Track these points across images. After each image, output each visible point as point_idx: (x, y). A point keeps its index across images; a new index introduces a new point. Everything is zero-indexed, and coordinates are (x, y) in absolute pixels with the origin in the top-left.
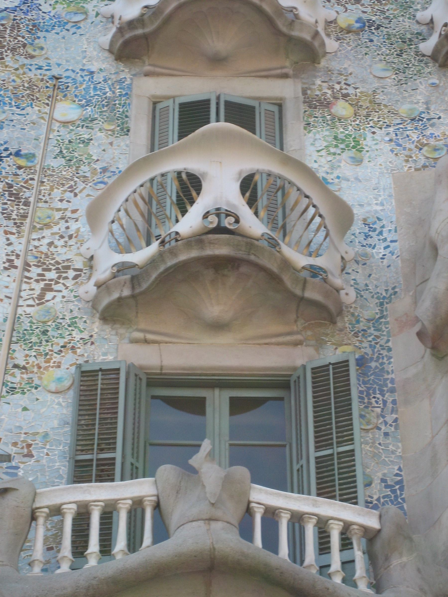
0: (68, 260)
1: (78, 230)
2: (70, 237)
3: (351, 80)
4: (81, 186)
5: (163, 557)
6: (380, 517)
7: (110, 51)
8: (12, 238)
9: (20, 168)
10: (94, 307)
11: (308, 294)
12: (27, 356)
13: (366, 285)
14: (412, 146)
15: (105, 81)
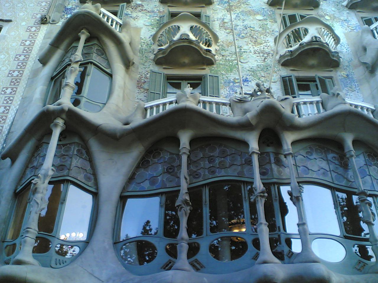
0: (269, 52)
1: (270, 45)
2: (268, 46)
3: (328, 11)
4: (268, 35)
5: (316, 119)
6: (375, 107)
7: (267, 3)
8: (254, 47)
9: (252, 30)
10: (279, 62)
11: (334, 59)
12: (264, 74)
13: (344, 58)
14: (346, 27)
15: (268, 10)
